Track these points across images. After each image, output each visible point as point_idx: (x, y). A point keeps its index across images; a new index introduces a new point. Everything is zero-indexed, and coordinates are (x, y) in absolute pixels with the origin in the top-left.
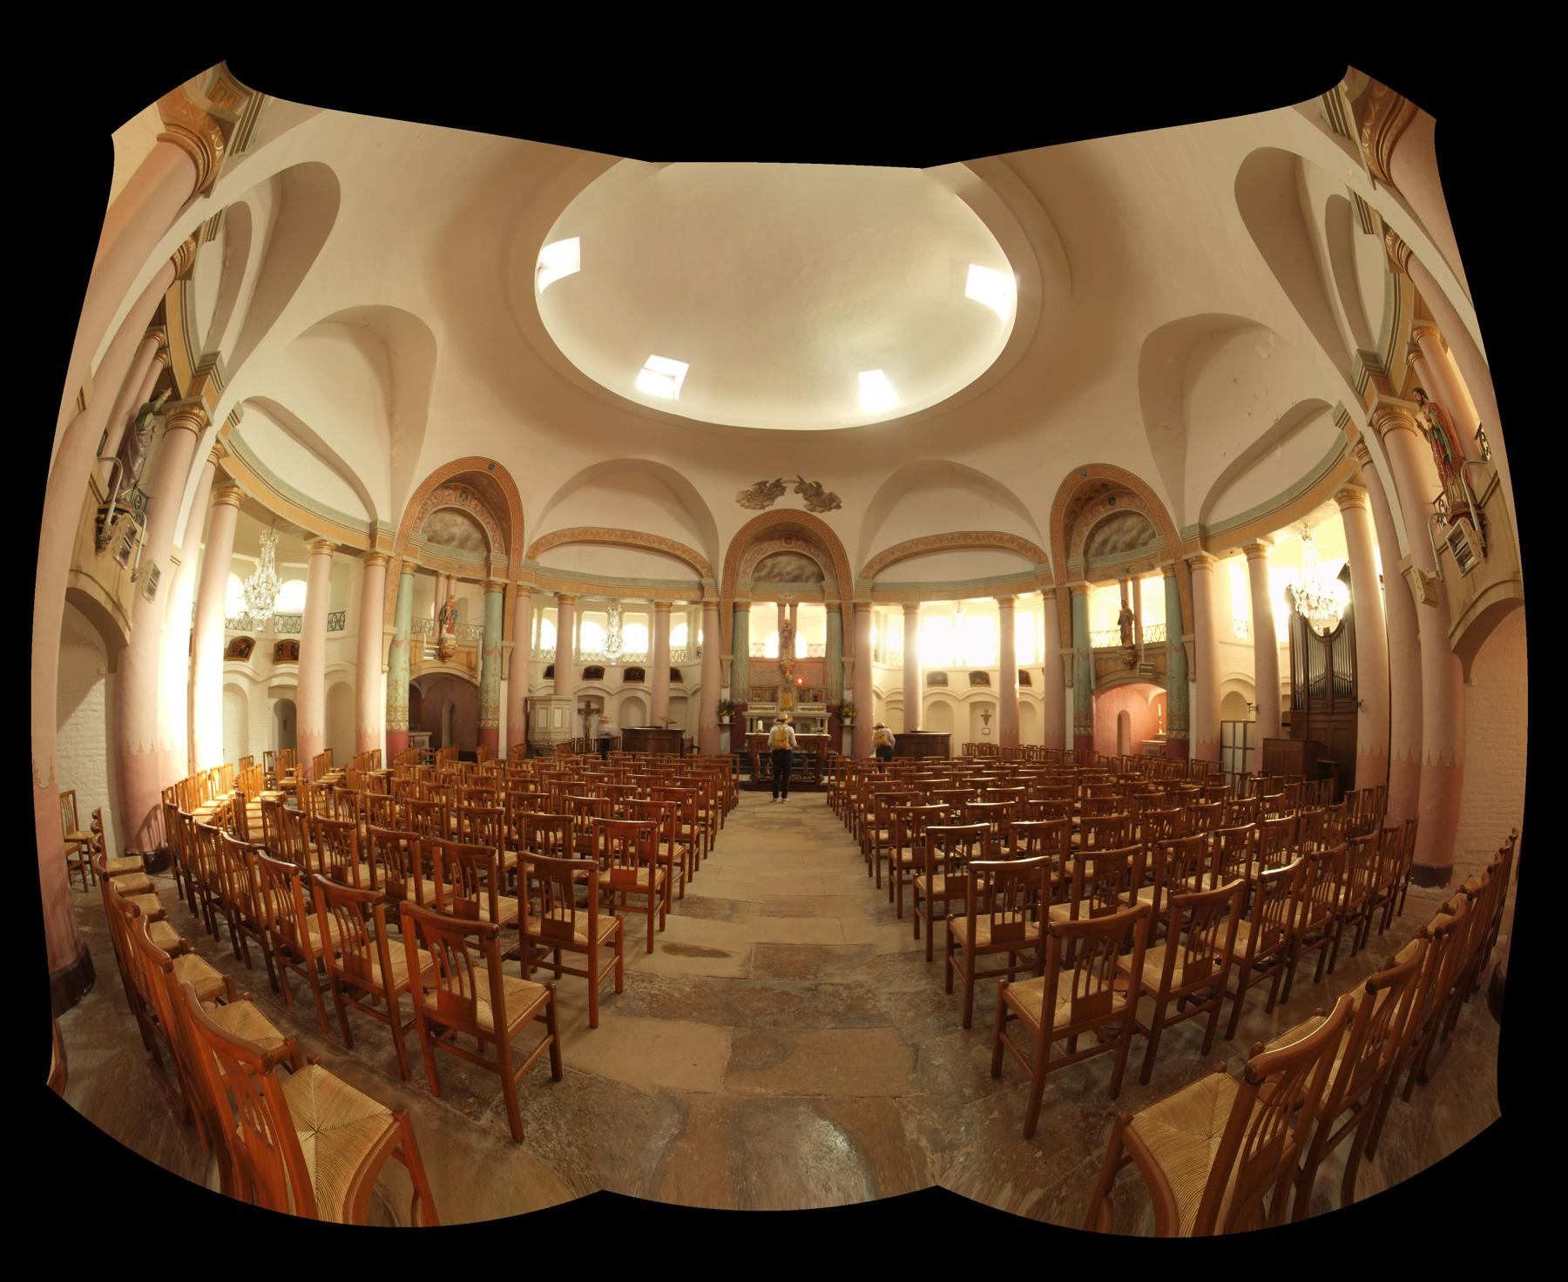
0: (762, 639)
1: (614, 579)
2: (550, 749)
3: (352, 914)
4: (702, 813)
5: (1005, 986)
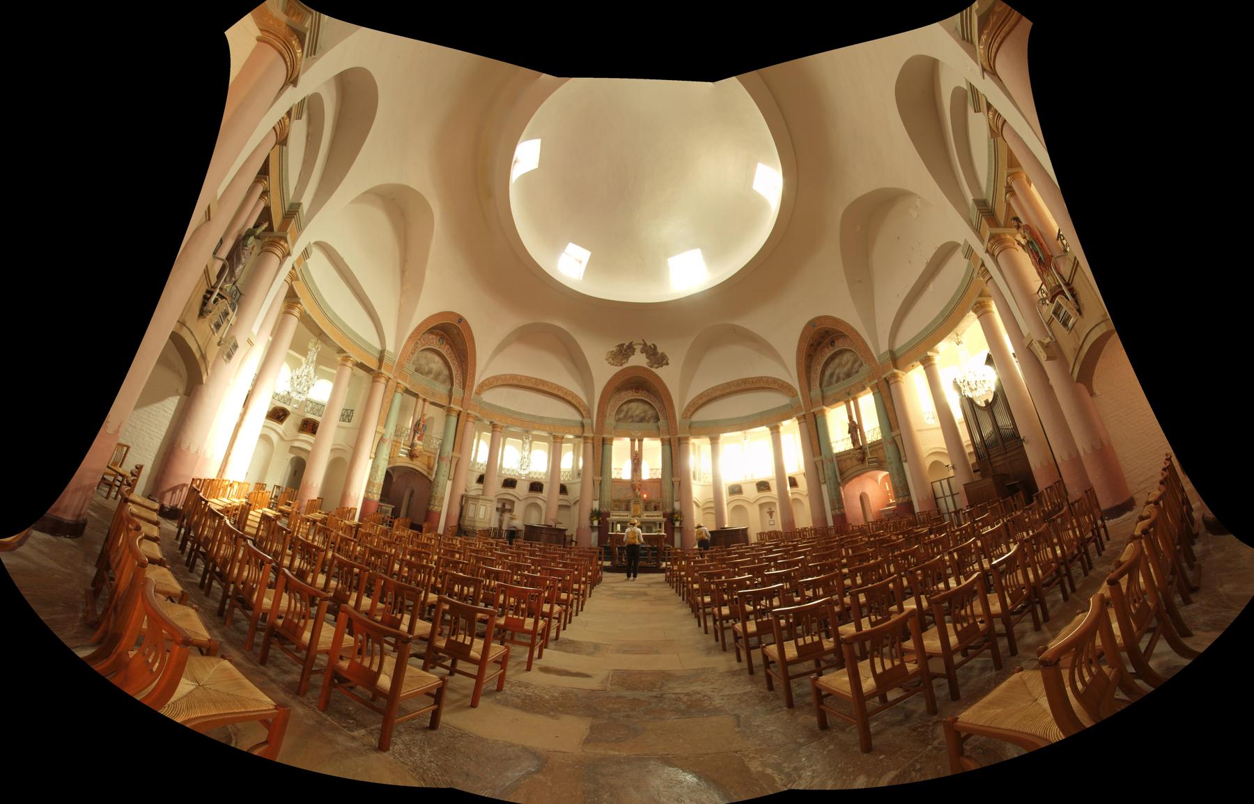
0: (621, 468)
2: (474, 532)
3: (301, 599)
4: (576, 586)
5: (816, 679)
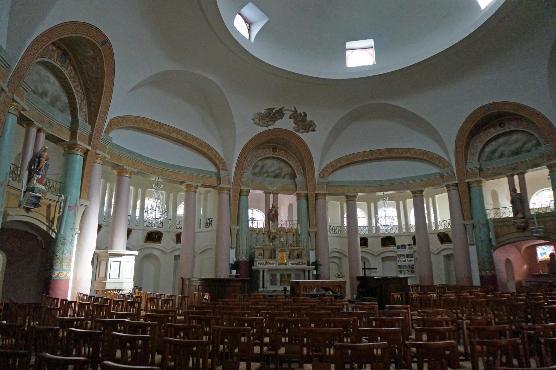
1: (160, 163)
